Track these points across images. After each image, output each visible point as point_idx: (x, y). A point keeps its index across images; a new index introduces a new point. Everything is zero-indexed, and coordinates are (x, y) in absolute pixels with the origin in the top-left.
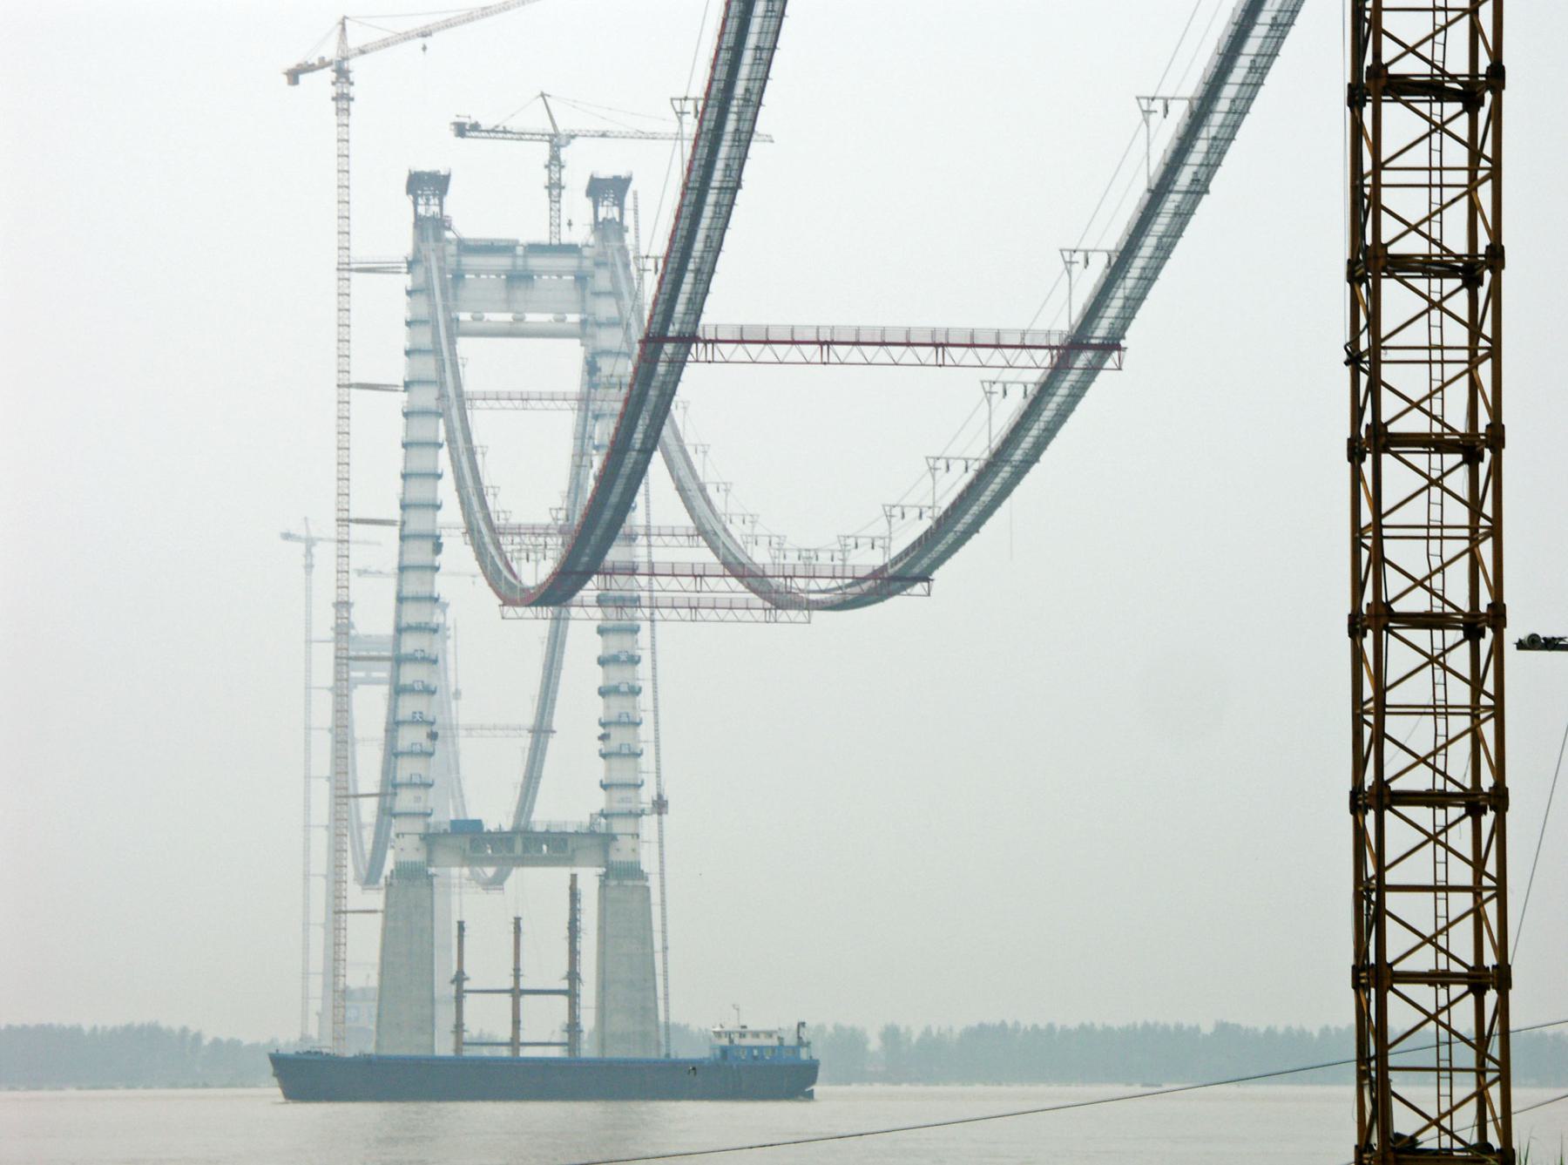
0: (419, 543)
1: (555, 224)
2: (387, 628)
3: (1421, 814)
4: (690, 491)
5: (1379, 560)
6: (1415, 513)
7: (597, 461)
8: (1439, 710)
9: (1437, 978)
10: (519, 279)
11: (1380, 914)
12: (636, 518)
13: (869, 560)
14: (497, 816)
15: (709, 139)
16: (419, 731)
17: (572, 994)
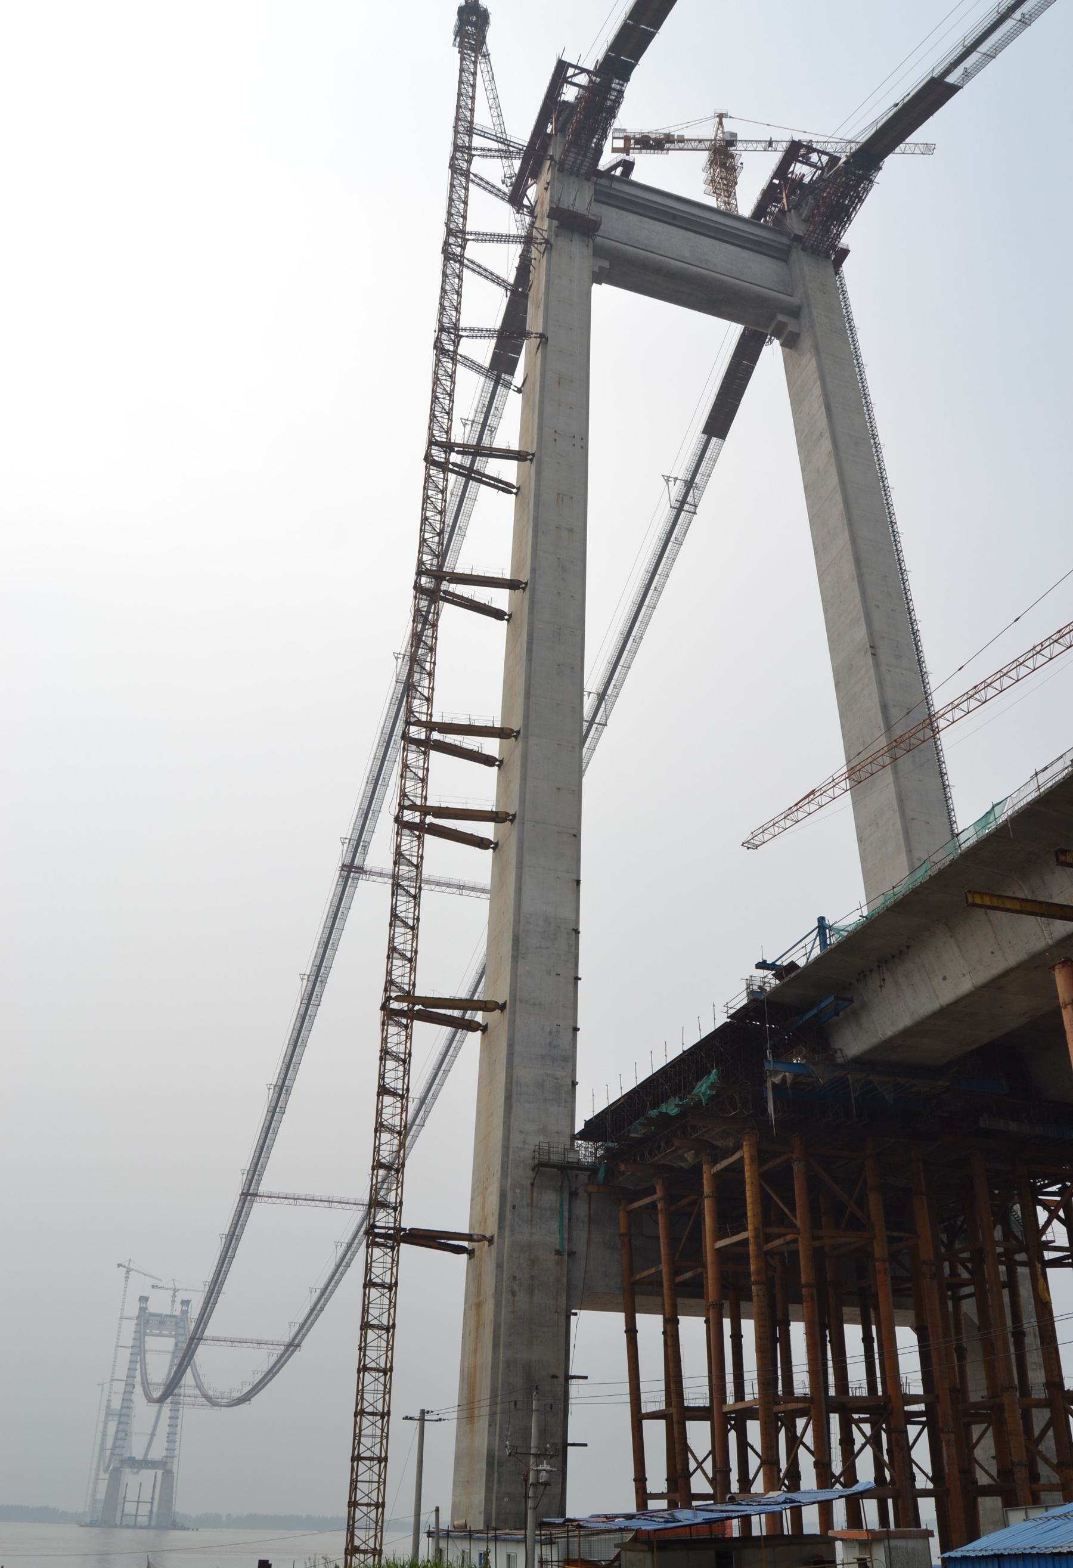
0: (130, 1386)
1: (172, 1311)
2: (119, 1407)
3: (367, 1462)
4: (196, 1376)
5: (362, 1398)
6: (371, 1387)
7: (175, 1368)
8: (373, 1436)
9: (368, 1505)
10: (162, 1323)
11: (356, 1488)
12: (183, 1382)
13: (236, 1395)
14: (139, 1455)
15: (211, 1292)
16: (123, 1433)
17: (152, 1503)
